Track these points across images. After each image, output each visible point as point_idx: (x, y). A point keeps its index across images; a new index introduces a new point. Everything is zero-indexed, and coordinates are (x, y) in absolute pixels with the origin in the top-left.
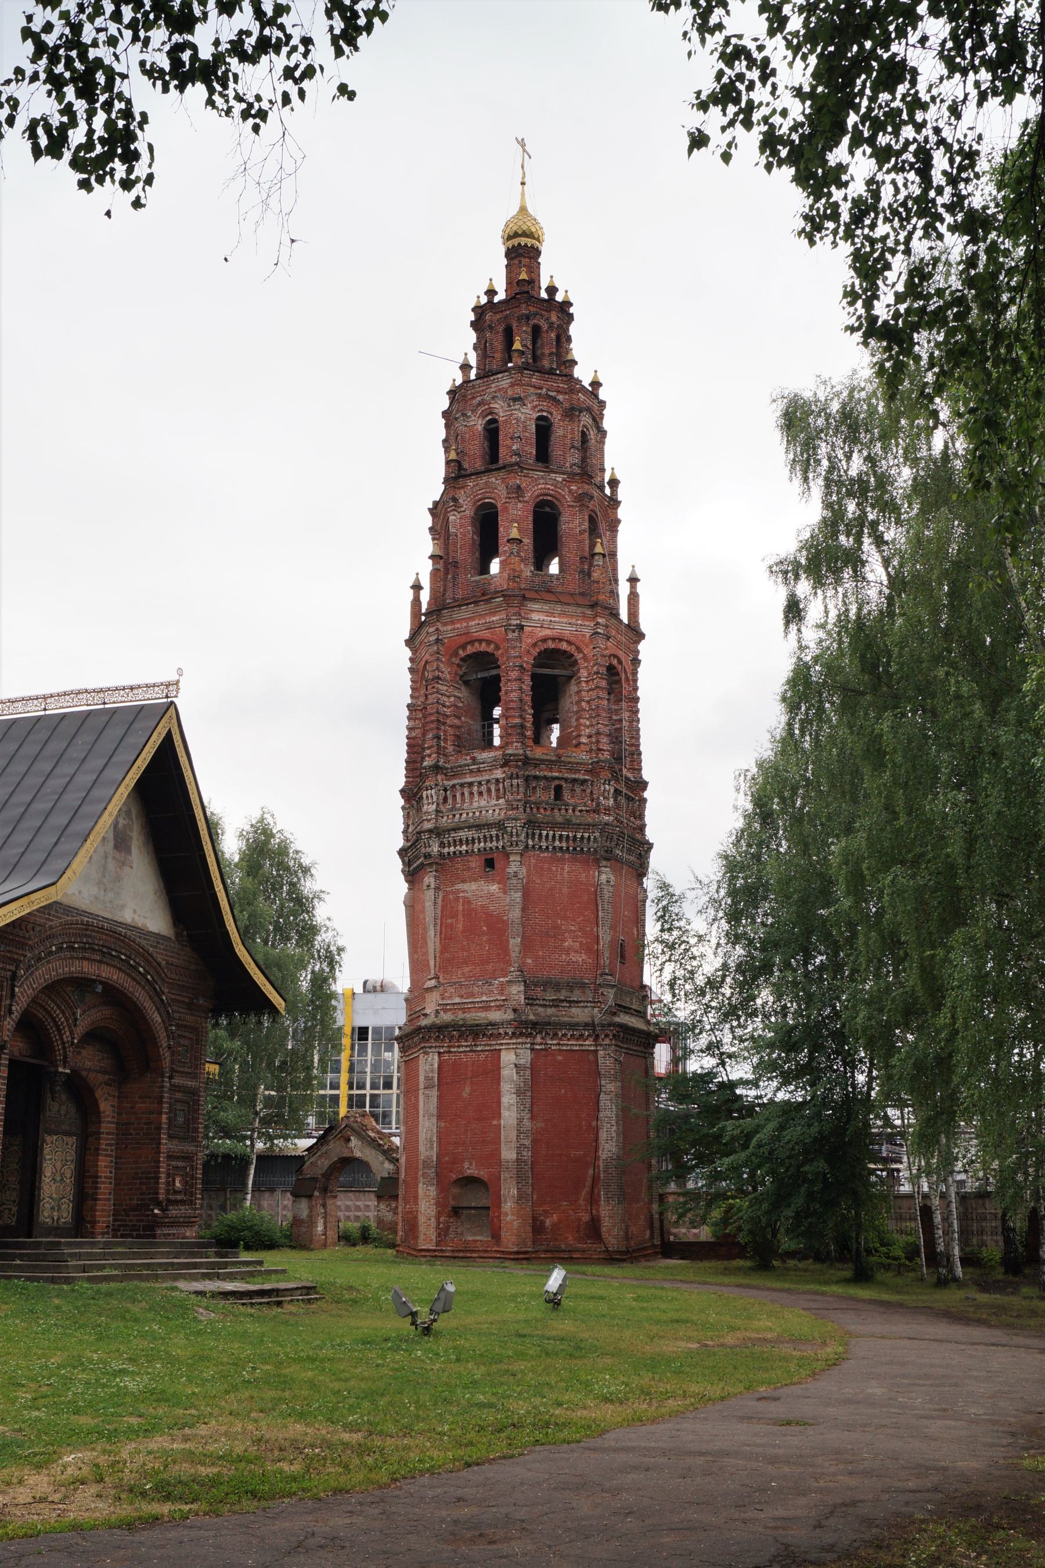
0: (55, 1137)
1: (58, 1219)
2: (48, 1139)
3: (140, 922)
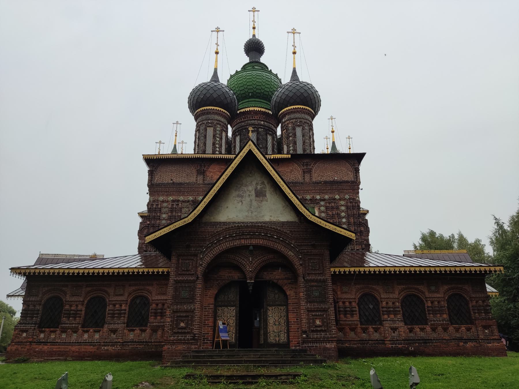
0: (274, 307)
1: (279, 340)
2: (270, 308)
3: (274, 219)
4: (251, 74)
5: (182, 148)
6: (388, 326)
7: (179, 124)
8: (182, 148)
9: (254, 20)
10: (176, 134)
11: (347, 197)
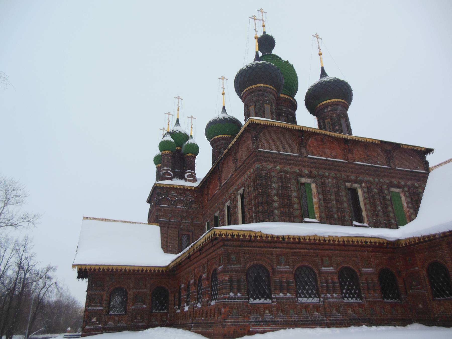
5: (191, 123)
7: (180, 99)
8: (191, 123)
9: (263, 19)
10: (178, 108)
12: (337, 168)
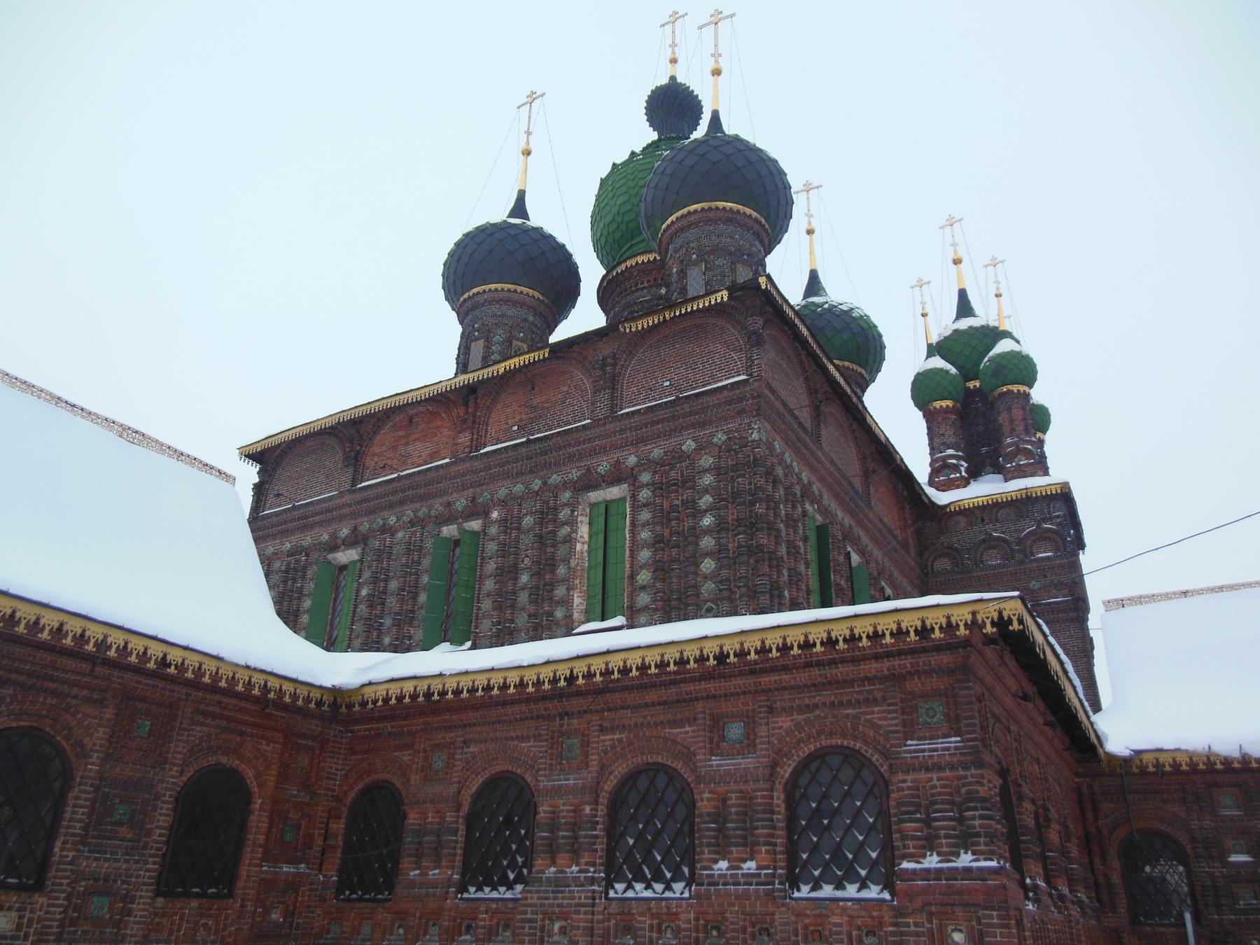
4: (624, 174)
6: (535, 905)
11: (720, 437)
12: (422, 491)
